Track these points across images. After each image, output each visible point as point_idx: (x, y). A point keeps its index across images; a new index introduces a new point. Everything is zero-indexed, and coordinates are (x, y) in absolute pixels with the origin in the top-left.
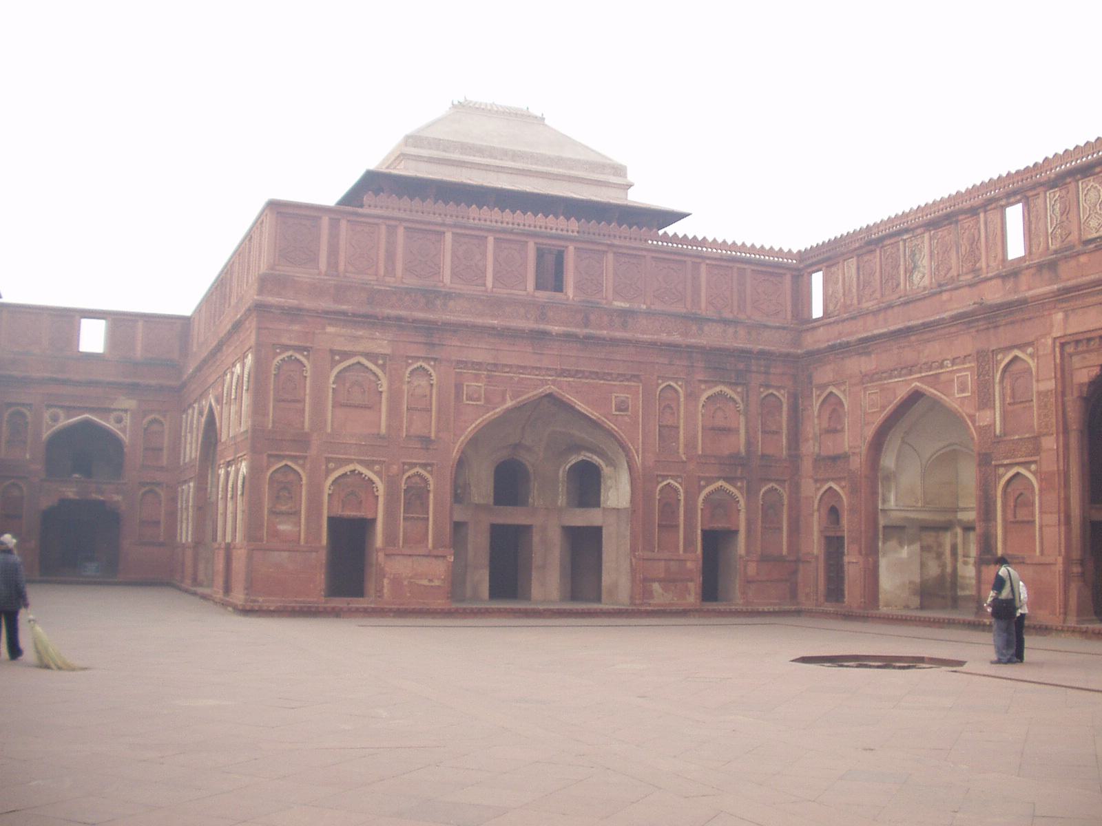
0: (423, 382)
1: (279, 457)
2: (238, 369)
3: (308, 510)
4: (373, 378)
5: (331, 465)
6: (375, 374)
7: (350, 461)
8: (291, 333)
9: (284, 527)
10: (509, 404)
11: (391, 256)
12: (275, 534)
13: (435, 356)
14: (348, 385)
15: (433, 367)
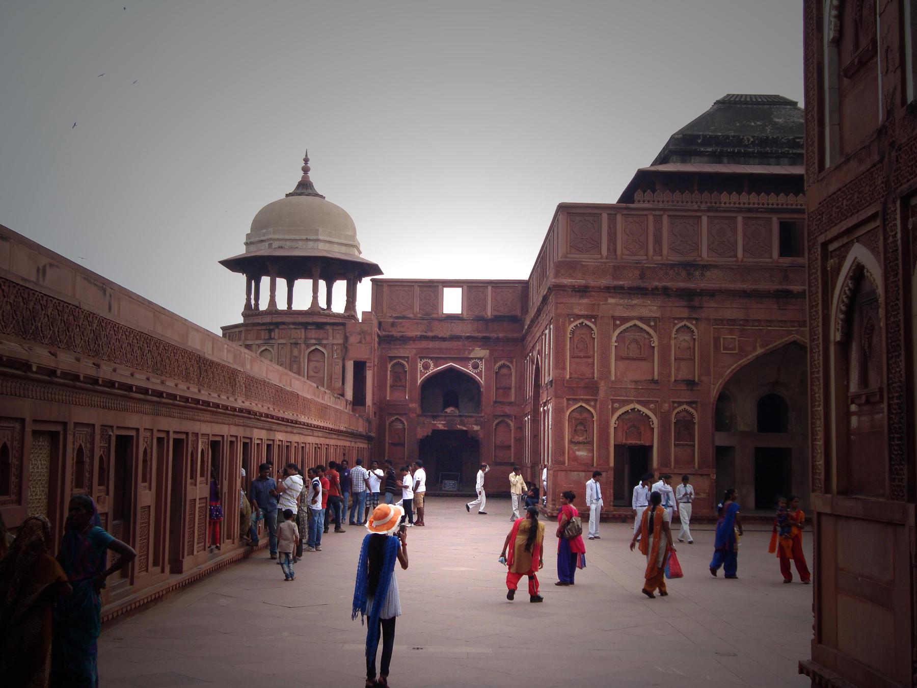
0: (688, 338)
1: (576, 400)
2: (547, 332)
3: (599, 440)
4: (646, 336)
5: (616, 405)
6: (648, 333)
7: (631, 402)
8: (581, 305)
9: (582, 453)
10: (759, 351)
11: (658, 240)
12: (575, 459)
13: (696, 316)
14: (627, 343)
15: (696, 325)
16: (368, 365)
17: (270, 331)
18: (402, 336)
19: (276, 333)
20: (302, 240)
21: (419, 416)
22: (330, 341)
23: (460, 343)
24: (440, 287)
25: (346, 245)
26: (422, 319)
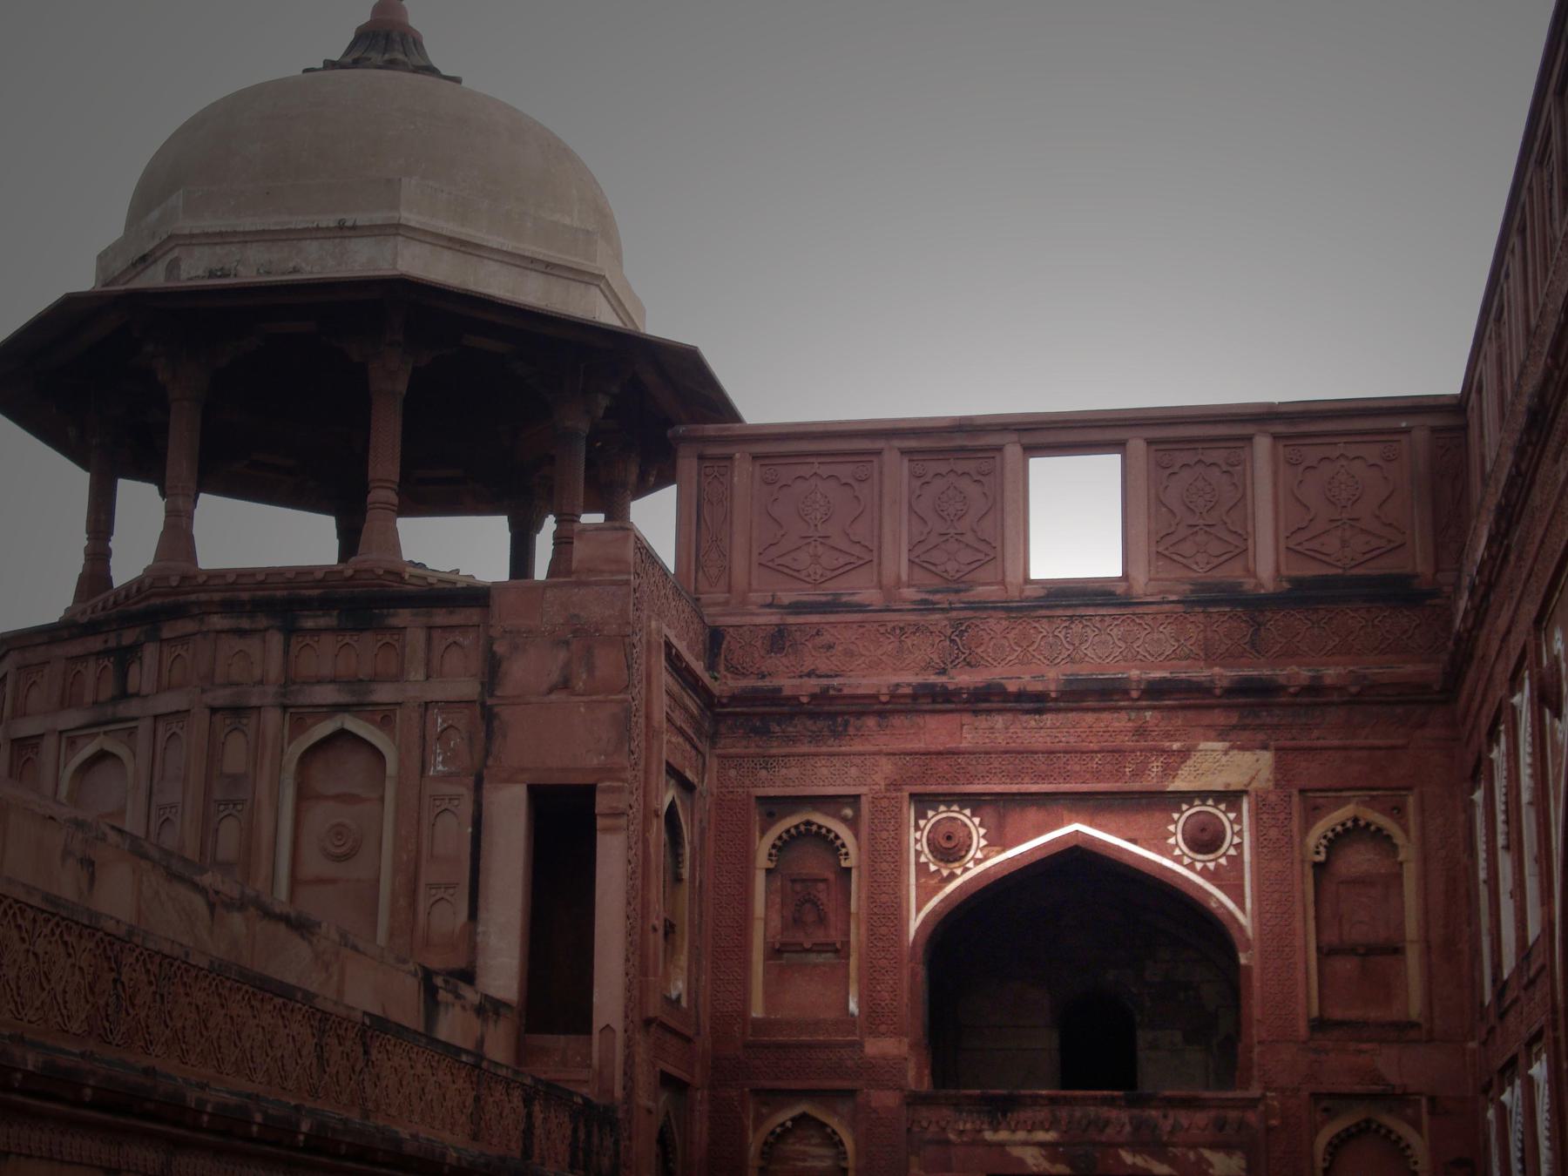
16: (602, 803)
17: (125, 657)
18: (822, 696)
19: (142, 676)
20: (315, 233)
21: (915, 1100)
22: (415, 687)
23: (1119, 722)
24: (1013, 451)
25: (549, 268)
26: (926, 607)
